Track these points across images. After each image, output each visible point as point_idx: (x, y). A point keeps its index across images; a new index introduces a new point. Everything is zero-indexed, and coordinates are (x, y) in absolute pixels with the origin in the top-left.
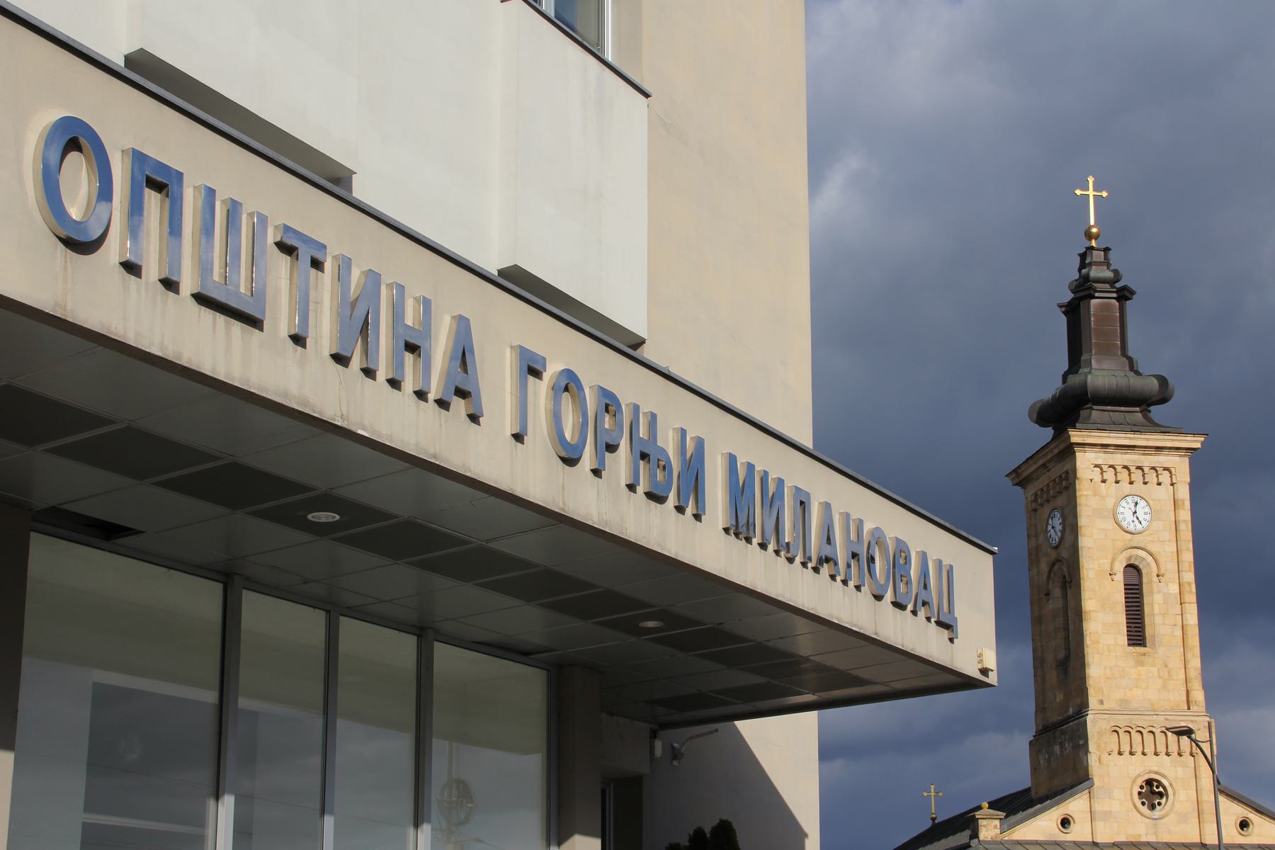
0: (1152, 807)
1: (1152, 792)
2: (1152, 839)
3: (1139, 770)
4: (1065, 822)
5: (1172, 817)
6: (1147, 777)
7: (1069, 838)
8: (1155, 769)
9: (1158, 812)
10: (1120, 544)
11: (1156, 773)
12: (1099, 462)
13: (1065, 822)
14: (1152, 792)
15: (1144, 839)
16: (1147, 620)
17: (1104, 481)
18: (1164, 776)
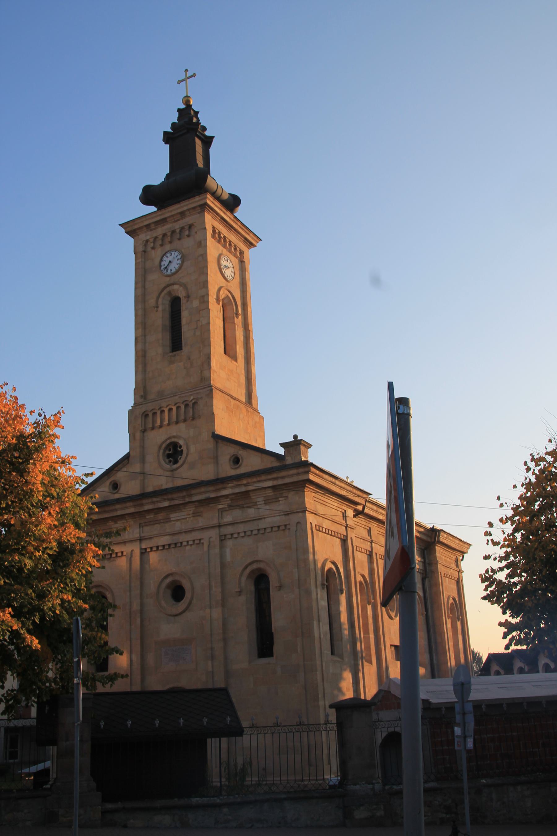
0: (176, 462)
1: (173, 452)
2: (170, 485)
3: (164, 438)
4: (115, 486)
5: (185, 466)
6: (168, 442)
8: (175, 434)
10: (163, 286)
11: (174, 437)
12: (148, 237)
13: (115, 486)
14: (173, 452)
15: (164, 487)
17: (153, 248)
18: (179, 437)
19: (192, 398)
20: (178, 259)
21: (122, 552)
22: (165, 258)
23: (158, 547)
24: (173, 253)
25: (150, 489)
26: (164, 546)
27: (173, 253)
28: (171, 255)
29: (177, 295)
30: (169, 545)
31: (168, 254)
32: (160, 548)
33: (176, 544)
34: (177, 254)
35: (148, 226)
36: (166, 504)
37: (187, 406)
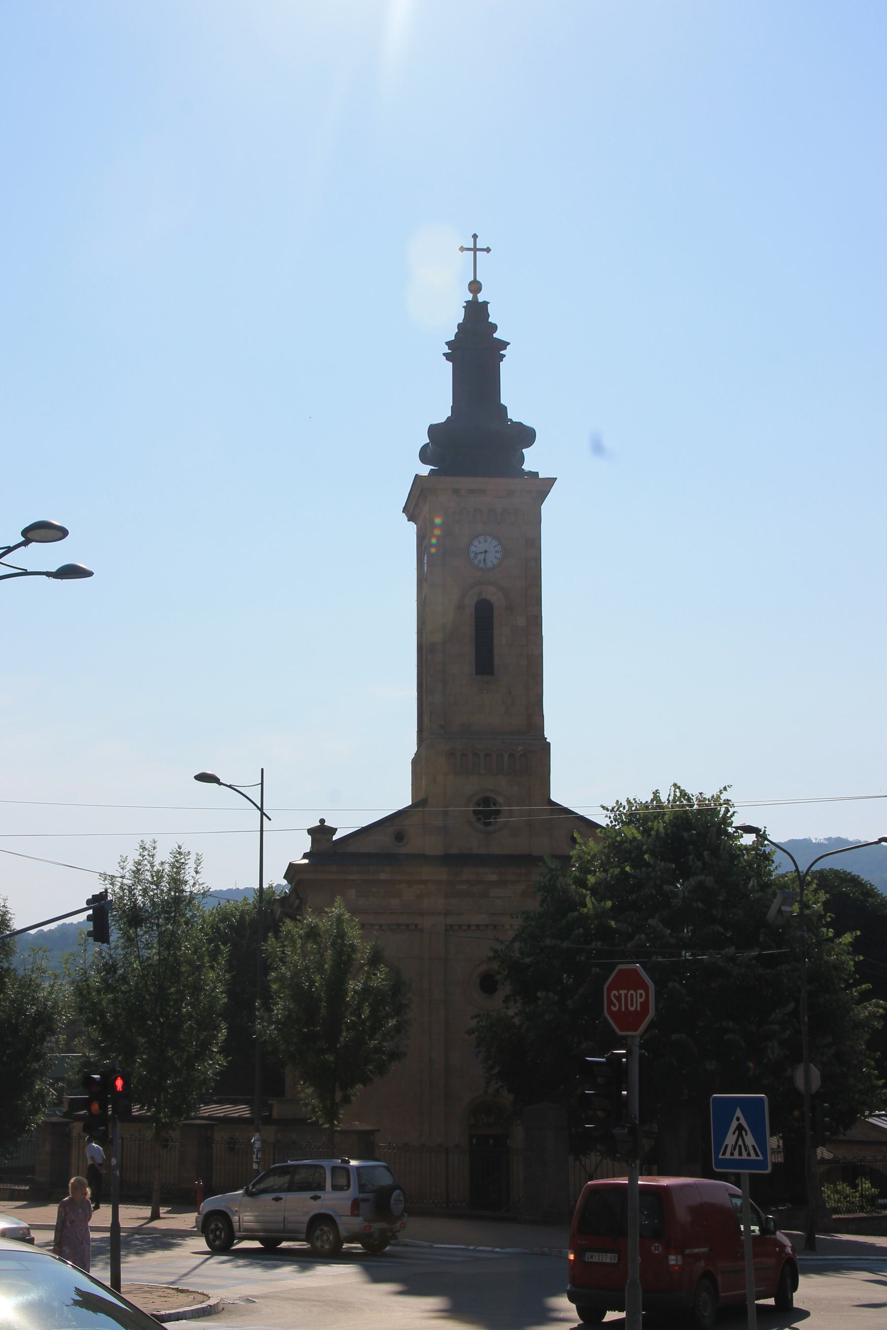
7: (404, 850)
9: (490, 828)
13: (399, 837)
16: (496, 651)
19: (520, 748)
20: (497, 552)
21: (416, 925)
22: (476, 543)
23: (469, 926)
24: (489, 540)
25: (454, 851)
26: (478, 926)
27: (489, 540)
28: (486, 541)
29: (488, 598)
30: (487, 926)
31: (482, 539)
32: (472, 928)
33: (495, 926)
34: (495, 543)
35: (456, 491)
36: (494, 878)
37: (511, 756)
